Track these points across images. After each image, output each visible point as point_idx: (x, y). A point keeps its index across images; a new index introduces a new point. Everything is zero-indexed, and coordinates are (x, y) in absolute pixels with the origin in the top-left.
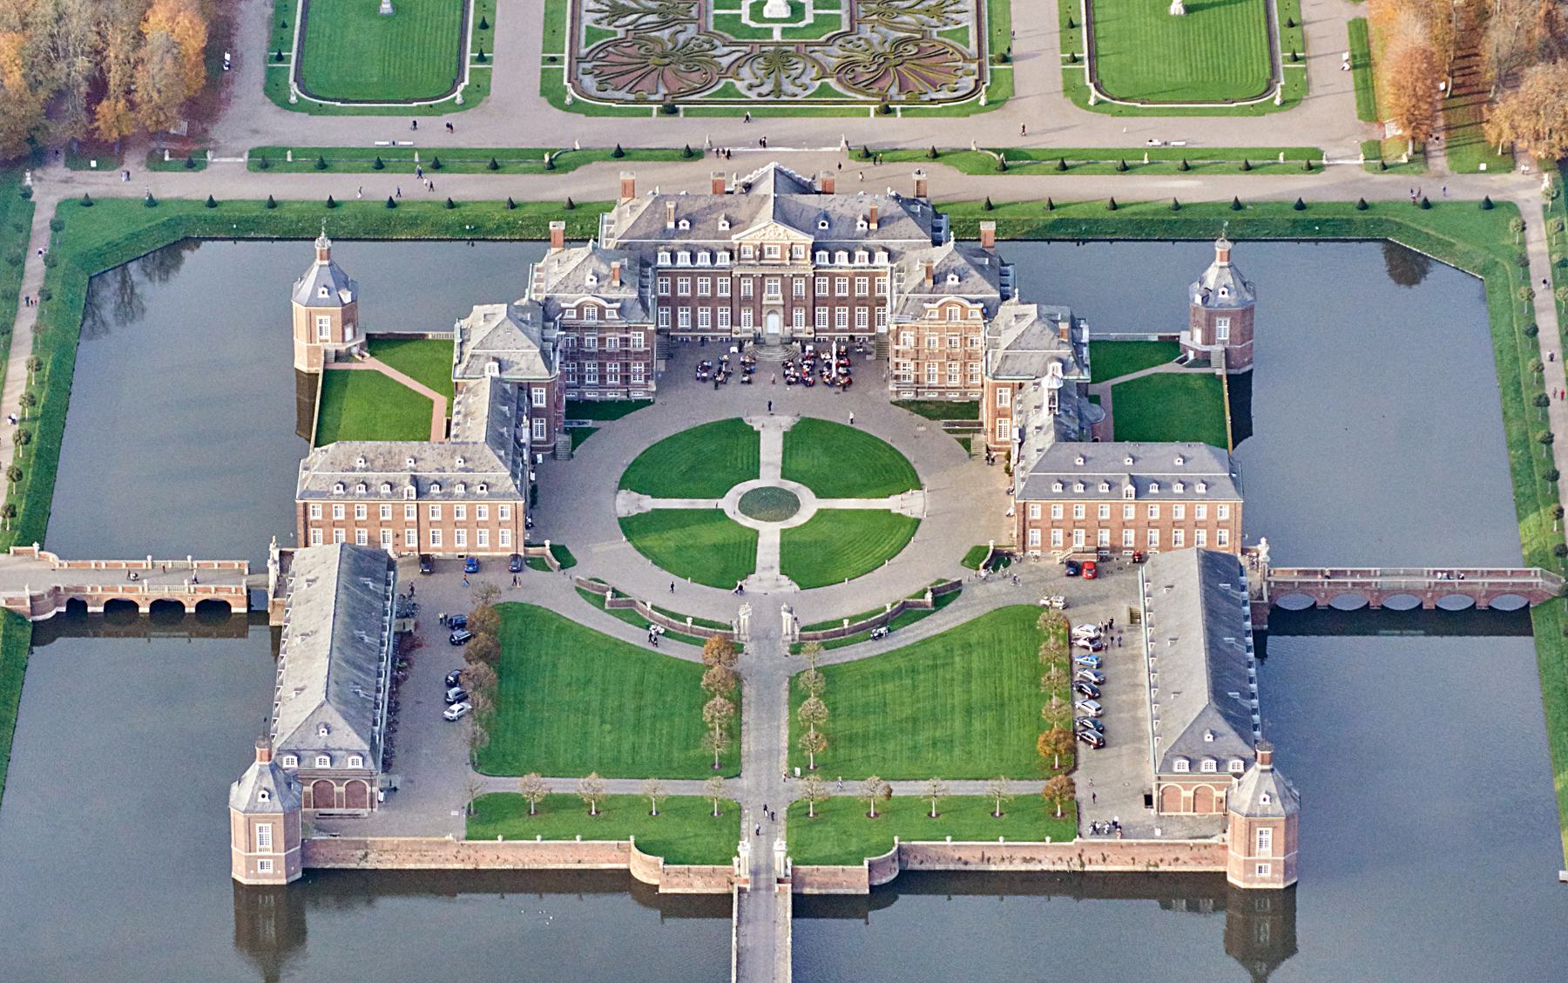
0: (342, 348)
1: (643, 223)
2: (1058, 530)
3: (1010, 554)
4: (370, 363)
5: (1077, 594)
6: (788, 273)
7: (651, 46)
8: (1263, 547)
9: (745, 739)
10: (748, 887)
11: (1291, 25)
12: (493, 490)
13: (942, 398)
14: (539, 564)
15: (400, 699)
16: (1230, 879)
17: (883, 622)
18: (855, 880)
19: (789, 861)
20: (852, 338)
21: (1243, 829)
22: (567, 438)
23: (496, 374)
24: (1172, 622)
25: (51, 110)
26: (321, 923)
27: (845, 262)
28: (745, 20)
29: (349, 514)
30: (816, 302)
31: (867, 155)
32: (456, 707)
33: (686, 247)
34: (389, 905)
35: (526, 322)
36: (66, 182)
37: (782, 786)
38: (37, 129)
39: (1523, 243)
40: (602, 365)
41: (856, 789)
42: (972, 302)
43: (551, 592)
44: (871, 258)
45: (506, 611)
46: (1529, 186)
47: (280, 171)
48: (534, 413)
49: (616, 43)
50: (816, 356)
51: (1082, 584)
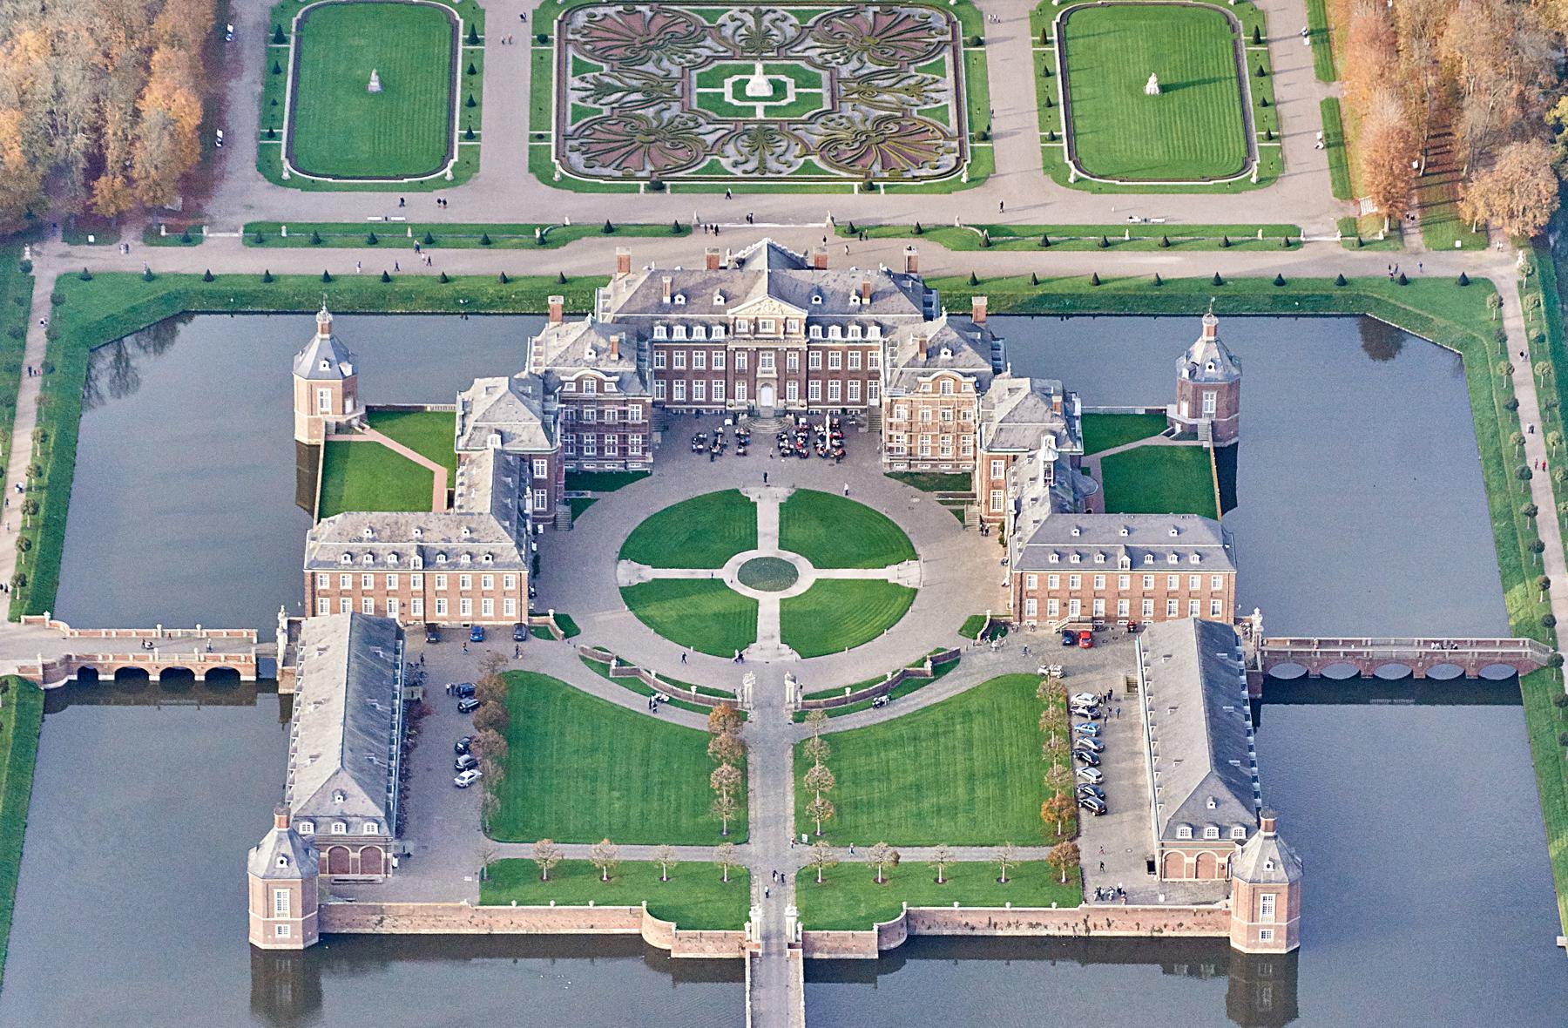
0: (343, 420)
1: (639, 298)
2: (1054, 601)
3: (1007, 624)
4: (371, 435)
5: (1072, 662)
6: (782, 346)
7: (636, 123)
8: (1256, 618)
9: (751, 805)
10: (760, 952)
11: (1265, 104)
12: (498, 560)
13: (935, 470)
14: (544, 633)
15: (411, 767)
16: (1233, 944)
17: (884, 691)
18: (864, 945)
19: (800, 926)
20: (844, 410)
22: (567, 509)
23: (499, 446)
24: (1171, 691)
26: (332, 986)
27: (838, 336)
28: (728, 98)
29: (356, 584)
30: (809, 375)
31: (853, 231)
32: (466, 774)
33: (682, 322)
34: (402, 969)
35: (527, 395)
36: (61, 256)
37: (790, 852)
38: (35, 204)
39: (1500, 319)
40: (600, 438)
41: (865, 856)
42: (965, 375)
43: (556, 661)
44: (864, 333)
45: (512, 678)
46: (1506, 262)
47: (276, 246)
48: (537, 484)
49: (601, 122)
50: (809, 429)
51: (1078, 654)
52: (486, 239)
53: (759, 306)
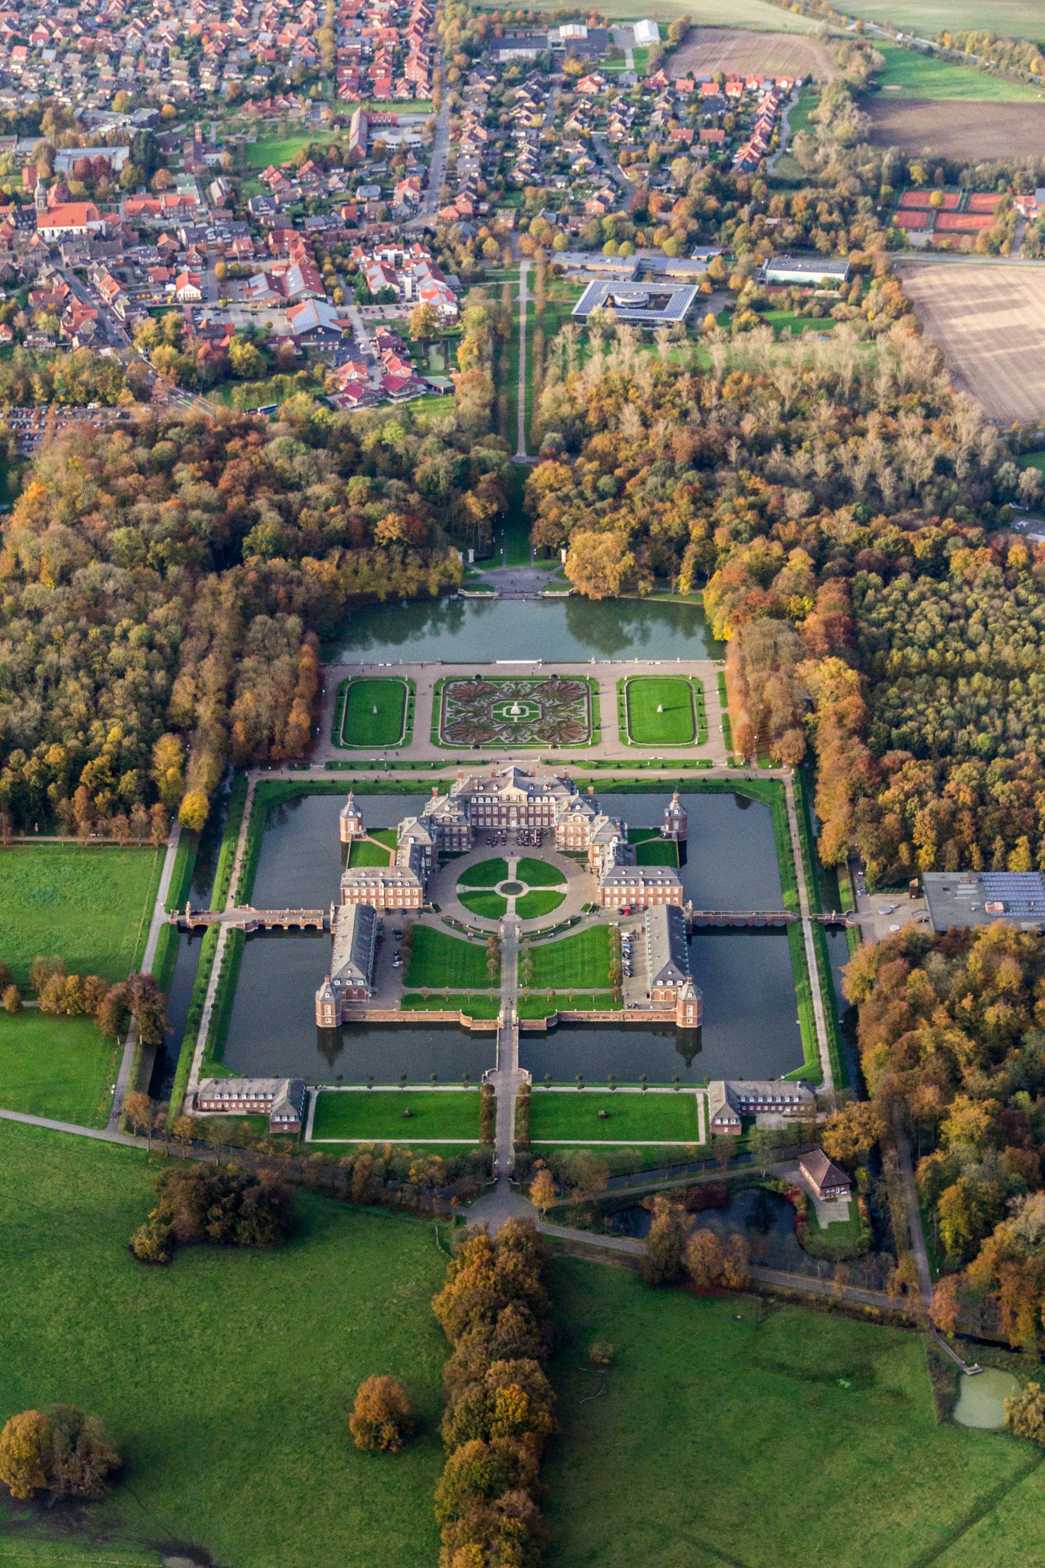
2: (616, 897)
14: (428, 911)
18: (542, 1024)
21: (680, 1004)
25: (256, 749)
34: (373, 1034)
43: (433, 921)
51: (625, 918)
52: (413, 766)
53: (511, 791)
